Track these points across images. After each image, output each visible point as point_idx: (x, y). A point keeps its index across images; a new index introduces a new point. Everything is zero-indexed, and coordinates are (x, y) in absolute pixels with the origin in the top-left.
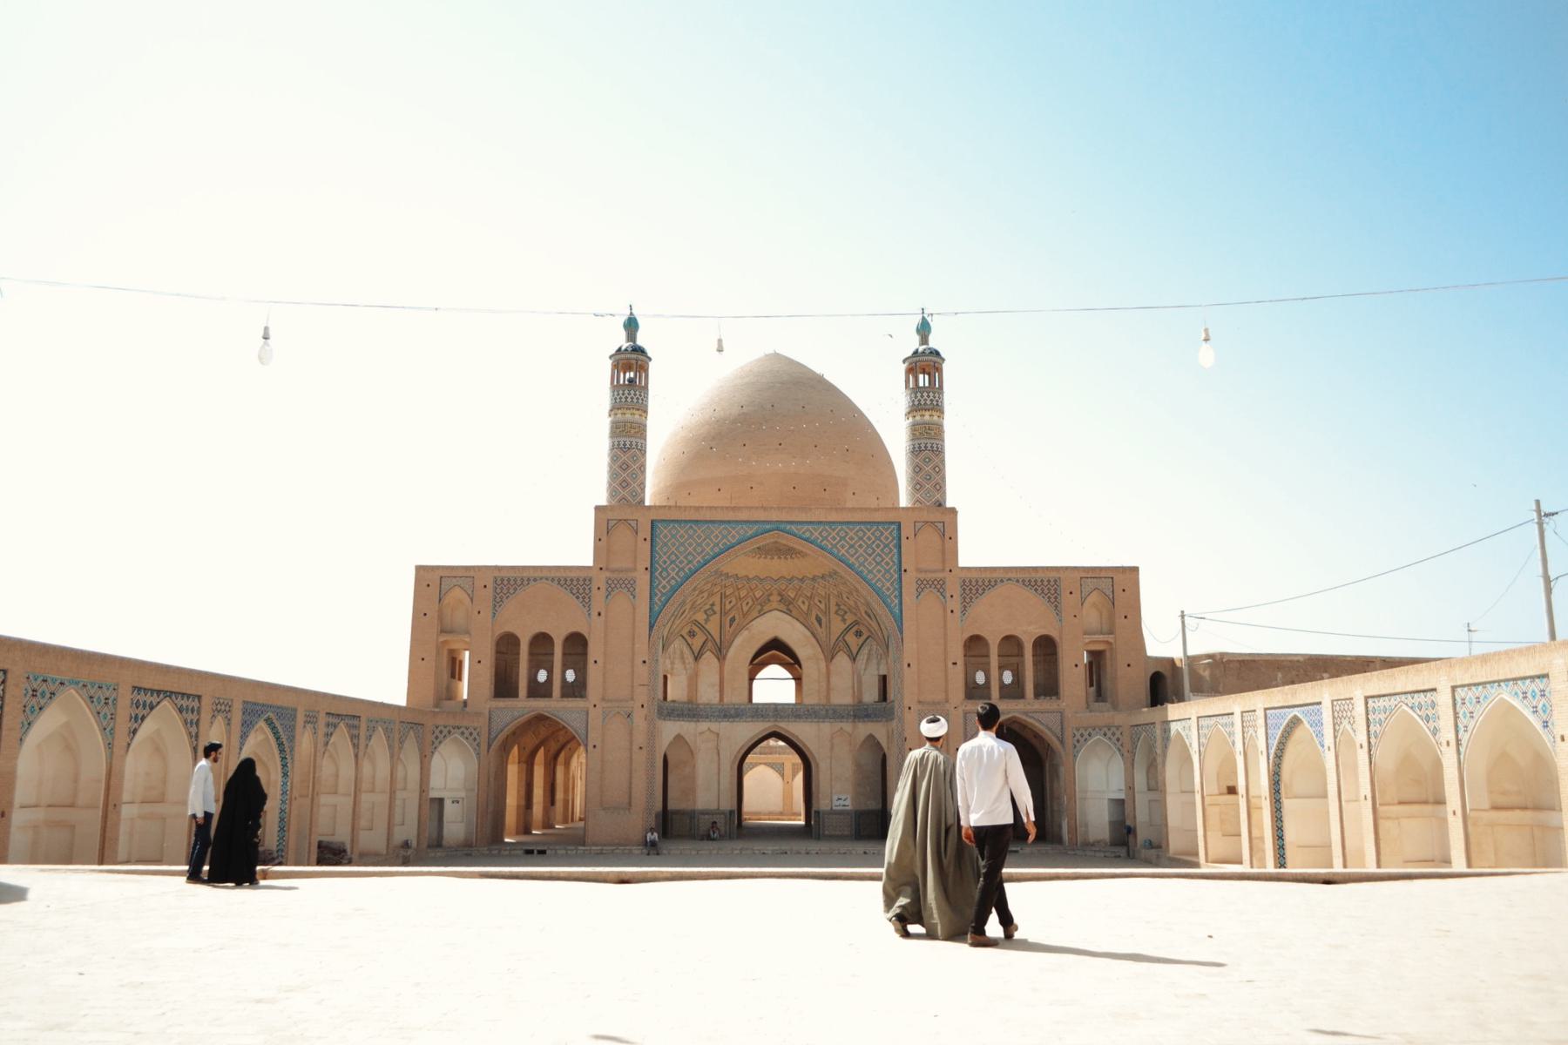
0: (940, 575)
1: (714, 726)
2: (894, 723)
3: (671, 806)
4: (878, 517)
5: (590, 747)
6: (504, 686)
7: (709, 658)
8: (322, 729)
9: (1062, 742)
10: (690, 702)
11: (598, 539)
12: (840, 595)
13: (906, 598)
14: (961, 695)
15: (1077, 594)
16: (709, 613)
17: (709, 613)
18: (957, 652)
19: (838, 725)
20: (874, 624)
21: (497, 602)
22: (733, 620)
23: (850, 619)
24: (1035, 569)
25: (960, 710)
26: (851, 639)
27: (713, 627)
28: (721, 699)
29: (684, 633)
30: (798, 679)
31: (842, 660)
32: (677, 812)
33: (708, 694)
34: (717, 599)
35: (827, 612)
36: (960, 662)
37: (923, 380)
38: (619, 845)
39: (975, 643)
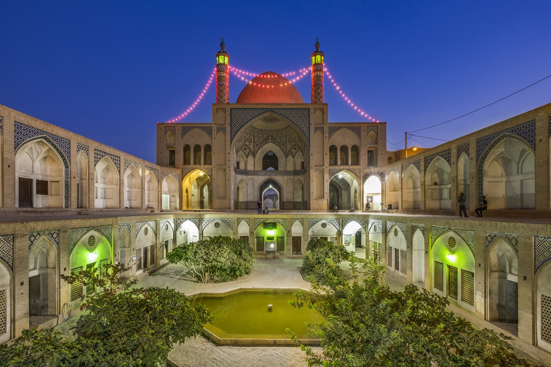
1: (252, 177)
6: (186, 162)
7: (251, 157)
10: (245, 170)
12: (290, 135)
13: (311, 133)
15: (366, 132)
18: (327, 150)
19: (289, 177)
20: (300, 144)
22: (257, 144)
23: (293, 143)
26: (293, 150)
27: (251, 147)
29: (243, 148)
31: (290, 158)
33: (250, 167)
34: (252, 137)
35: (286, 142)
39: (333, 149)
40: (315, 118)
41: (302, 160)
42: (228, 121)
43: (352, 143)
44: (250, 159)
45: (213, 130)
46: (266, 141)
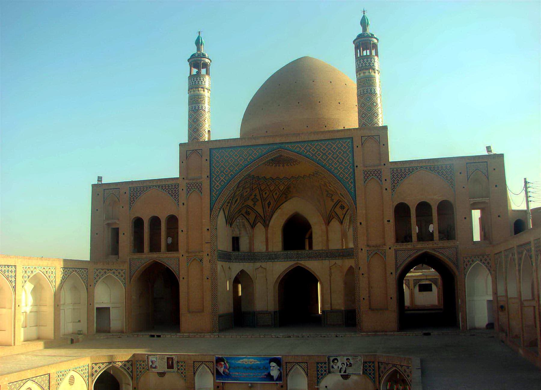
0: (379, 168)
1: (264, 265)
5: (181, 278)
6: (138, 247)
7: (259, 226)
9: (457, 266)
11: (181, 162)
14: (393, 240)
16: (255, 201)
17: (255, 201)
18: (390, 214)
19: (333, 262)
22: (269, 204)
26: (338, 210)
28: (267, 248)
31: (335, 224)
33: (260, 246)
36: (392, 220)
38: (198, 332)
42: (206, 173)
45: (180, 190)
46: (286, 195)
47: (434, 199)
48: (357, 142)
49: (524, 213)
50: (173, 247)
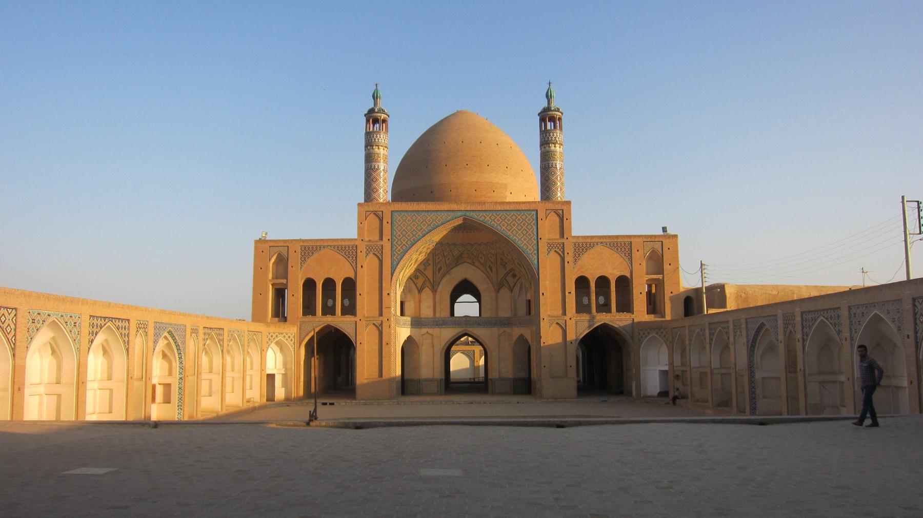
1: (430, 330)
2: (534, 328)
3: (406, 377)
4: (523, 207)
6: (309, 309)
8: (201, 336)
9: (632, 338)
18: (571, 286)
19: (502, 329)
20: (523, 270)
21: (304, 259)
22: (440, 269)
24: (617, 237)
25: (573, 321)
26: (510, 279)
27: (429, 273)
30: (479, 301)
31: (505, 292)
32: (410, 380)
33: (427, 312)
36: (573, 292)
37: (549, 125)
40: (548, 229)
41: (529, 298)
43: (618, 273)
44: (427, 294)
45: (359, 252)
46: (458, 261)
47: (613, 273)
48: (541, 215)
49: (698, 291)
50: (350, 309)
